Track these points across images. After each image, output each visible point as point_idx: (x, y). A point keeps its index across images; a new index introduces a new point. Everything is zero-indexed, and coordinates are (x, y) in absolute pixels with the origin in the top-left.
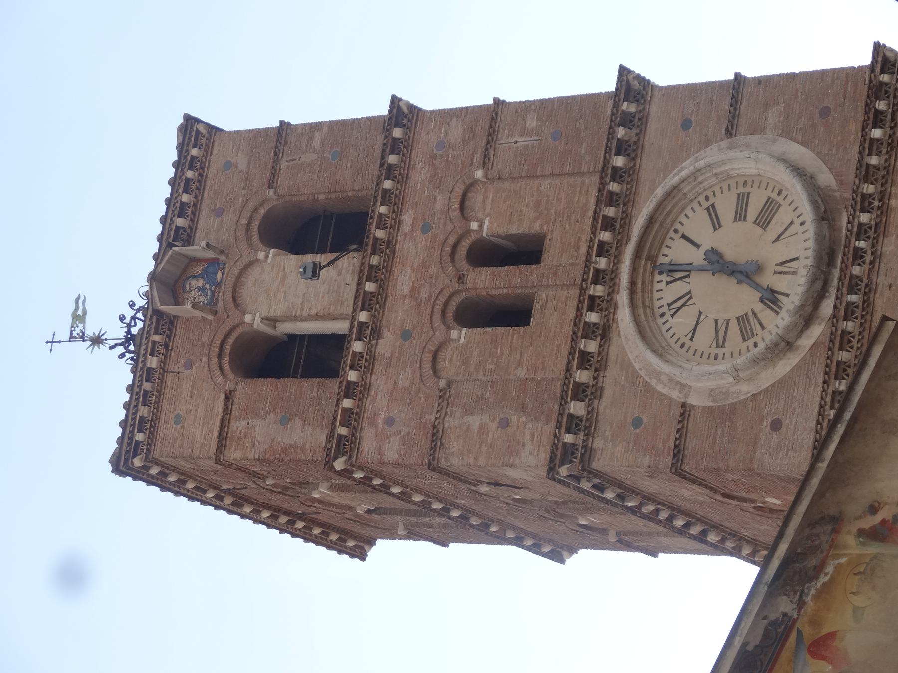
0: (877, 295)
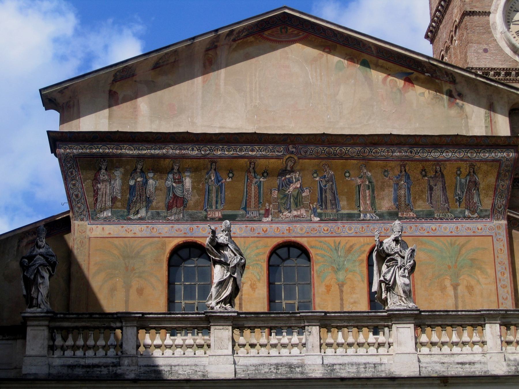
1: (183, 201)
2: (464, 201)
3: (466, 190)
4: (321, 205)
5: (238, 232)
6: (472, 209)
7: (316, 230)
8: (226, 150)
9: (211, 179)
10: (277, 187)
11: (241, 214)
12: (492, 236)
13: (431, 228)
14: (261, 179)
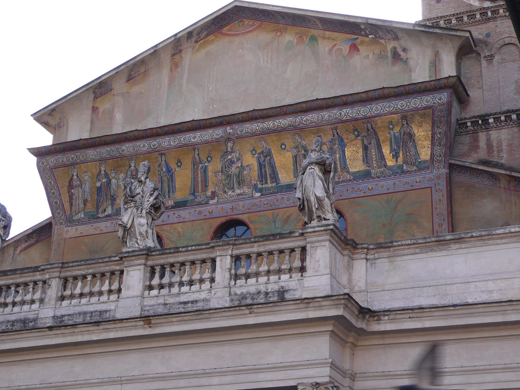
0: (493, 22)
2: (401, 155)
3: (401, 144)
5: (187, 216)
7: (257, 206)
8: (171, 141)
9: (163, 170)
12: (431, 187)
13: (367, 188)
14: (206, 164)
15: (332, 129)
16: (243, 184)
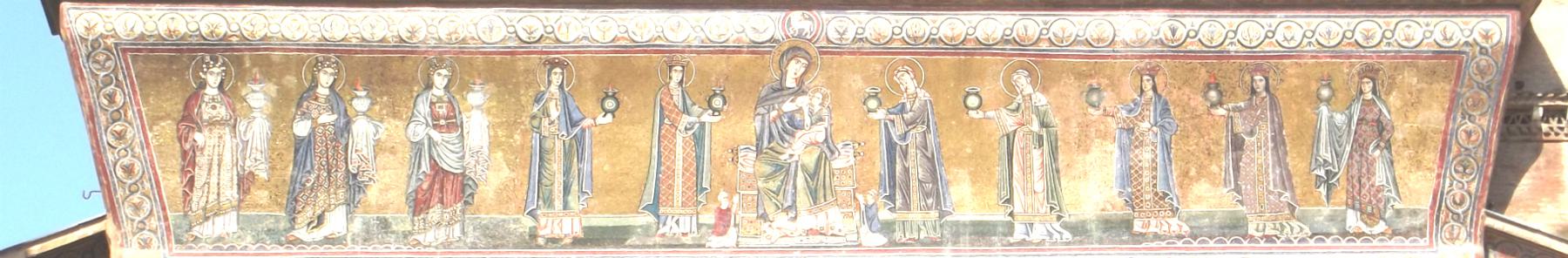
1: (463, 186)
2: (1343, 182)
3: (1348, 149)
4: (891, 198)
6: (1369, 209)
9: (549, 116)
10: (754, 140)
11: (641, 227)
15: (1140, 73)
16: (829, 198)
